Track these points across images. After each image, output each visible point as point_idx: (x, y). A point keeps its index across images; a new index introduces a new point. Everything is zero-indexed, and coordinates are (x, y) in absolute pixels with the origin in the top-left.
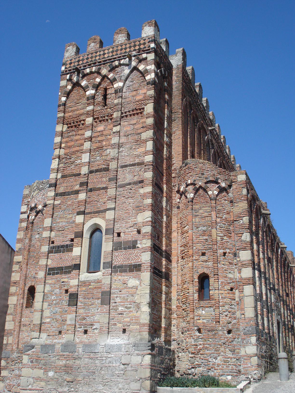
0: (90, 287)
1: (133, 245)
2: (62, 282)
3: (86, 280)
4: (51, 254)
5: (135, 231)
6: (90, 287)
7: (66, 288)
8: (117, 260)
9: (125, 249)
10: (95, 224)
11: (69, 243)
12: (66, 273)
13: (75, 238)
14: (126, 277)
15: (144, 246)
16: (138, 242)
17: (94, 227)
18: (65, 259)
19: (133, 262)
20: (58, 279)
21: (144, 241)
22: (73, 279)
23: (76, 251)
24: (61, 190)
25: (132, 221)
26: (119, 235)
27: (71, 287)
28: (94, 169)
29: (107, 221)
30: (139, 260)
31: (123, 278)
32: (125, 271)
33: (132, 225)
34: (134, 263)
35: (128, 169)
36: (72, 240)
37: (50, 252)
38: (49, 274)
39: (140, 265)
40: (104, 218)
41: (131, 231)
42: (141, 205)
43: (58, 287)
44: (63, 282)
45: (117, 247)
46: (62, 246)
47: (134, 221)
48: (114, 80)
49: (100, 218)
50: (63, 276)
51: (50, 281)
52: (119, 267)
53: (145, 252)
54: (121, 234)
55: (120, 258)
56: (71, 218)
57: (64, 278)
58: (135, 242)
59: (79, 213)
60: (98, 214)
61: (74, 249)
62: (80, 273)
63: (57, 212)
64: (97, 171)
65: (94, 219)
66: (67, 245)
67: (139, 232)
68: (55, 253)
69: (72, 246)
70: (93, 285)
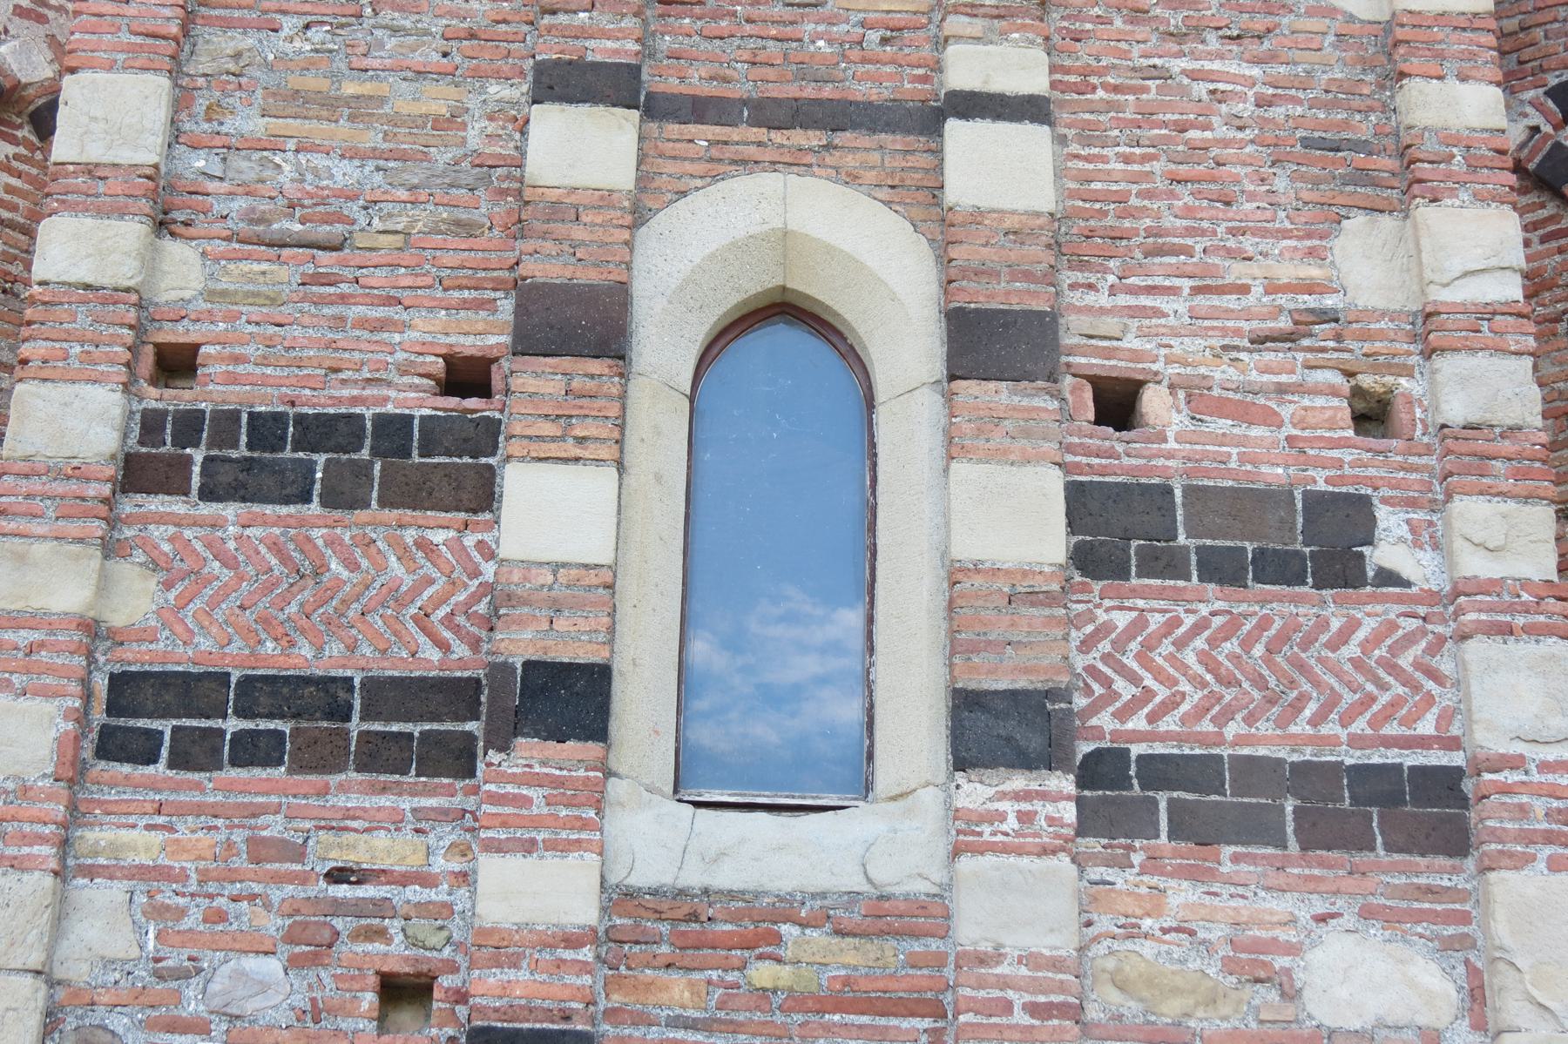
0: (763, 973)
1: (1327, 546)
2: (338, 876)
3: (693, 878)
4: (156, 504)
5: (1334, 392)
6: (763, 973)
7: (395, 953)
8: (1125, 690)
9: (1222, 569)
11: (417, 401)
12: (381, 757)
13: (528, 343)
14: (1280, 905)
15: (1475, 565)
16: (1389, 520)
17: (754, 283)
18: (371, 592)
19: (1345, 744)
20: (274, 827)
21: (1473, 514)
22: (529, 847)
23: (550, 511)
25: (1272, 289)
26: (1117, 405)
27: (498, 948)
30: (1426, 727)
31: (1227, 903)
32: (1256, 829)
33: (1284, 323)
34: (1356, 741)
36: (466, 377)
37: (140, 473)
38: (113, 746)
39: (1443, 787)
41: (1282, 390)
42: (1364, 128)
43: (273, 925)
44: (338, 876)
45: (1115, 532)
46: (326, 431)
47: (1310, 288)
49: (852, 179)
50: (350, 791)
51: (141, 843)
52: (1159, 772)
53: (1507, 631)
54: (1154, 402)
55: (1174, 668)
56: (453, 121)
57: (381, 825)
59: (564, 83)
60: (815, 138)
61: (519, 483)
62: (616, 788)
63: (227, 25)
65: (769, 182)
66: (393, 431)
67: (1372, 415)
68: (207, 494)
69: (487, 436)
70: (811, 956)
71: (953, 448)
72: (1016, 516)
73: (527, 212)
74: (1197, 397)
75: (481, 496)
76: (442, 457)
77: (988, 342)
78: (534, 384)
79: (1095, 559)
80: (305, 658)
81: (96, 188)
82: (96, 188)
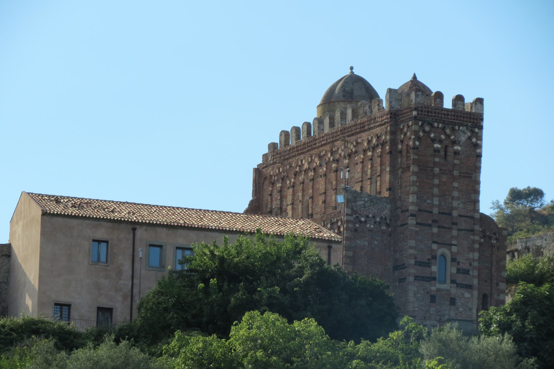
9: (463, 273)
10: (444, 252)
23: (434, 268)
24: (419, 220)
28: (441, 211)
29: (451, 252)
35: (463, 219)
36: (429, 260)
40: (450, 250)
46: (423, 263)
48: (454, 143)
58: (468, 271)
64: (443, 213)
71: (451, 266)
72: (454, 270)
73: (432, 250)
74: (462, 263)
75: (430, 267)
76: (428, 265)
77: (453, 260)
78: (433, 261)
79: (457, 272)
80: (423, 275)
81: (411, 247)
82: (411, 247)
